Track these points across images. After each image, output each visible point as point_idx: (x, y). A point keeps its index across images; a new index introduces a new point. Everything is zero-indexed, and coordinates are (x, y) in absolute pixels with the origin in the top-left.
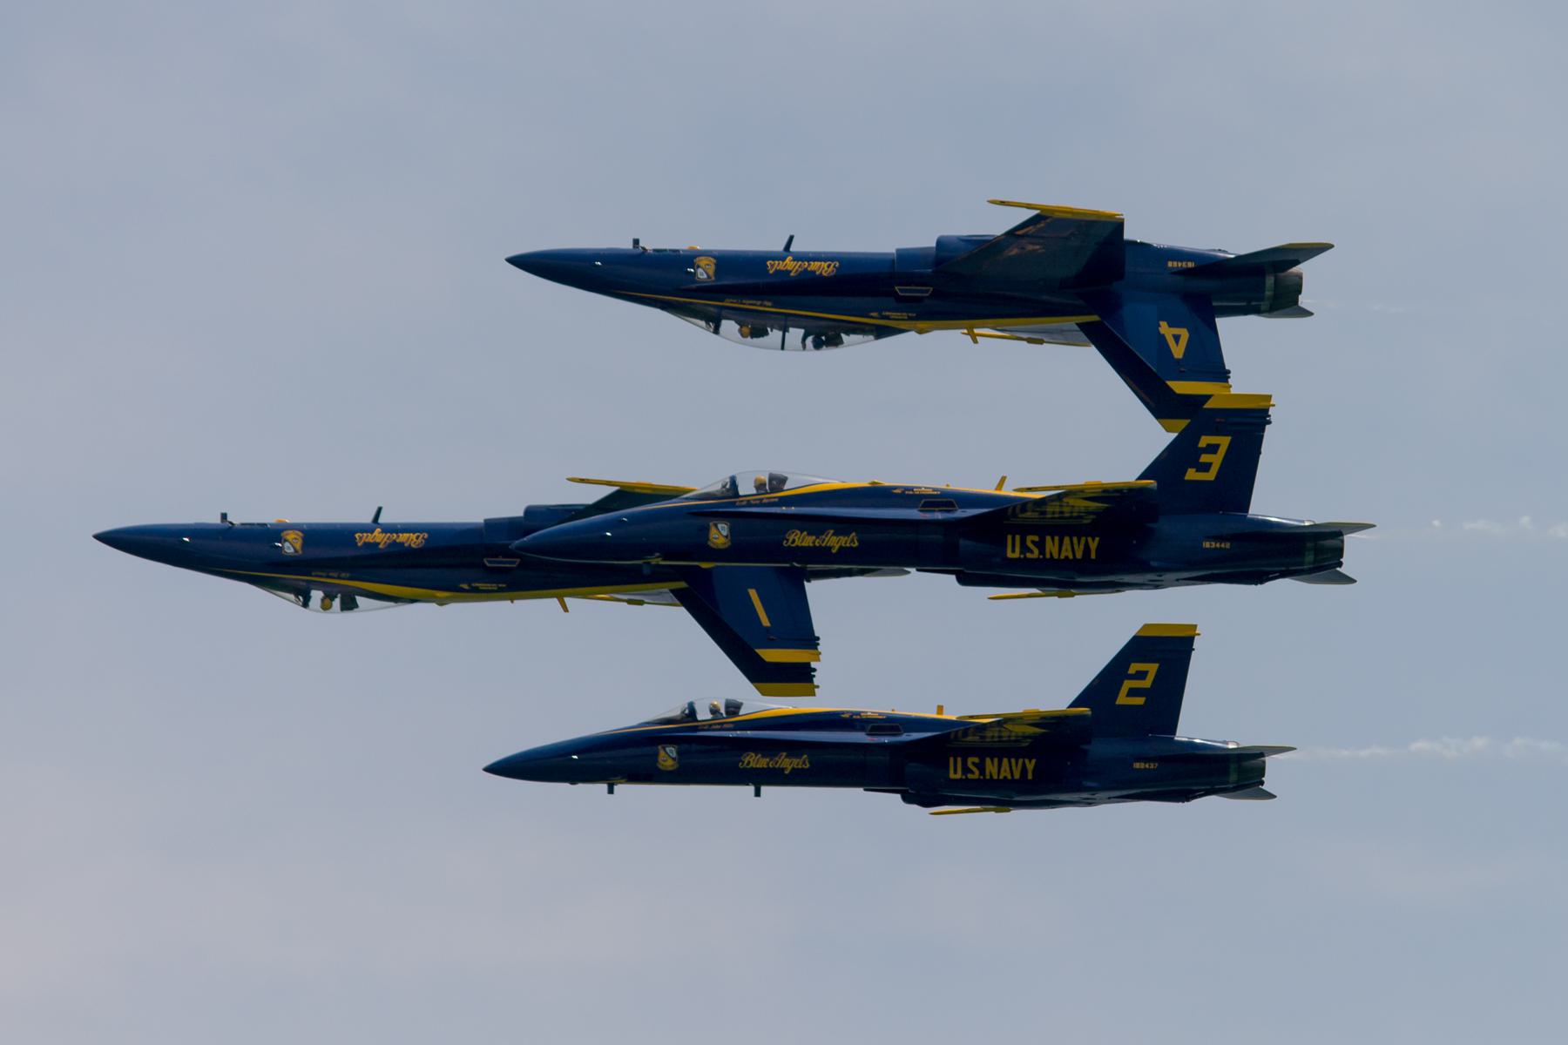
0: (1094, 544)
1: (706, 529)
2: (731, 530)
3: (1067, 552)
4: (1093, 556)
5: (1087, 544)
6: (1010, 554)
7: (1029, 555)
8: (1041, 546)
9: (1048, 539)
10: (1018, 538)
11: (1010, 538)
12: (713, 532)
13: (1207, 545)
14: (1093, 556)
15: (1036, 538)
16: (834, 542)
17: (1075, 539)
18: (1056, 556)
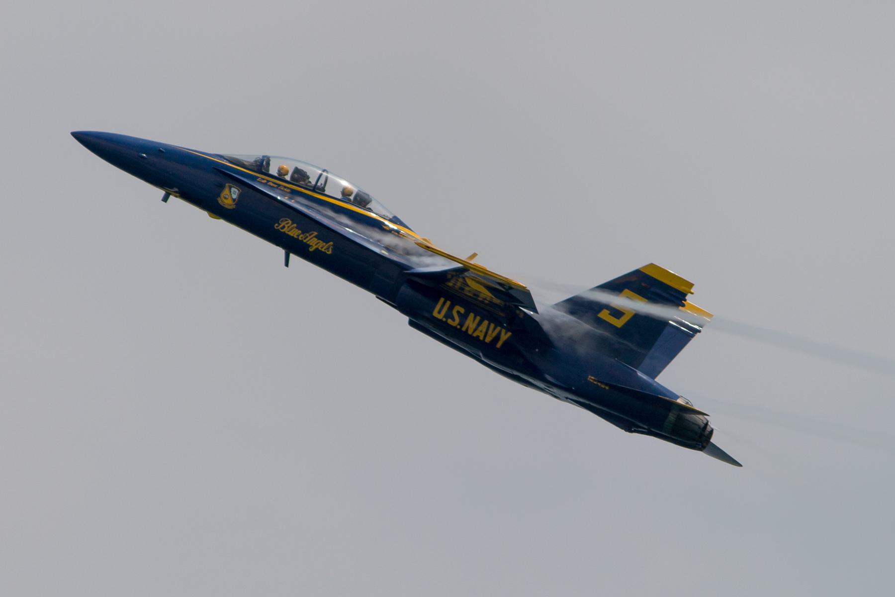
0: (505, 336)
1: (221, 187)
2: (240, 196)
3: (480, 334)
4: (499, 345)
5: (500, 333)
6: (435, 314)
7: (450, 321)
8: (463, 317)
9: (472, 315)
10: (448, 303)
11: (442, 300)
12: (226, 192)
13: (591, 378)
14: (499, 345)
15: (462, 310)
16: (314, 243)
17: (492, 325)
18: (470, 332)
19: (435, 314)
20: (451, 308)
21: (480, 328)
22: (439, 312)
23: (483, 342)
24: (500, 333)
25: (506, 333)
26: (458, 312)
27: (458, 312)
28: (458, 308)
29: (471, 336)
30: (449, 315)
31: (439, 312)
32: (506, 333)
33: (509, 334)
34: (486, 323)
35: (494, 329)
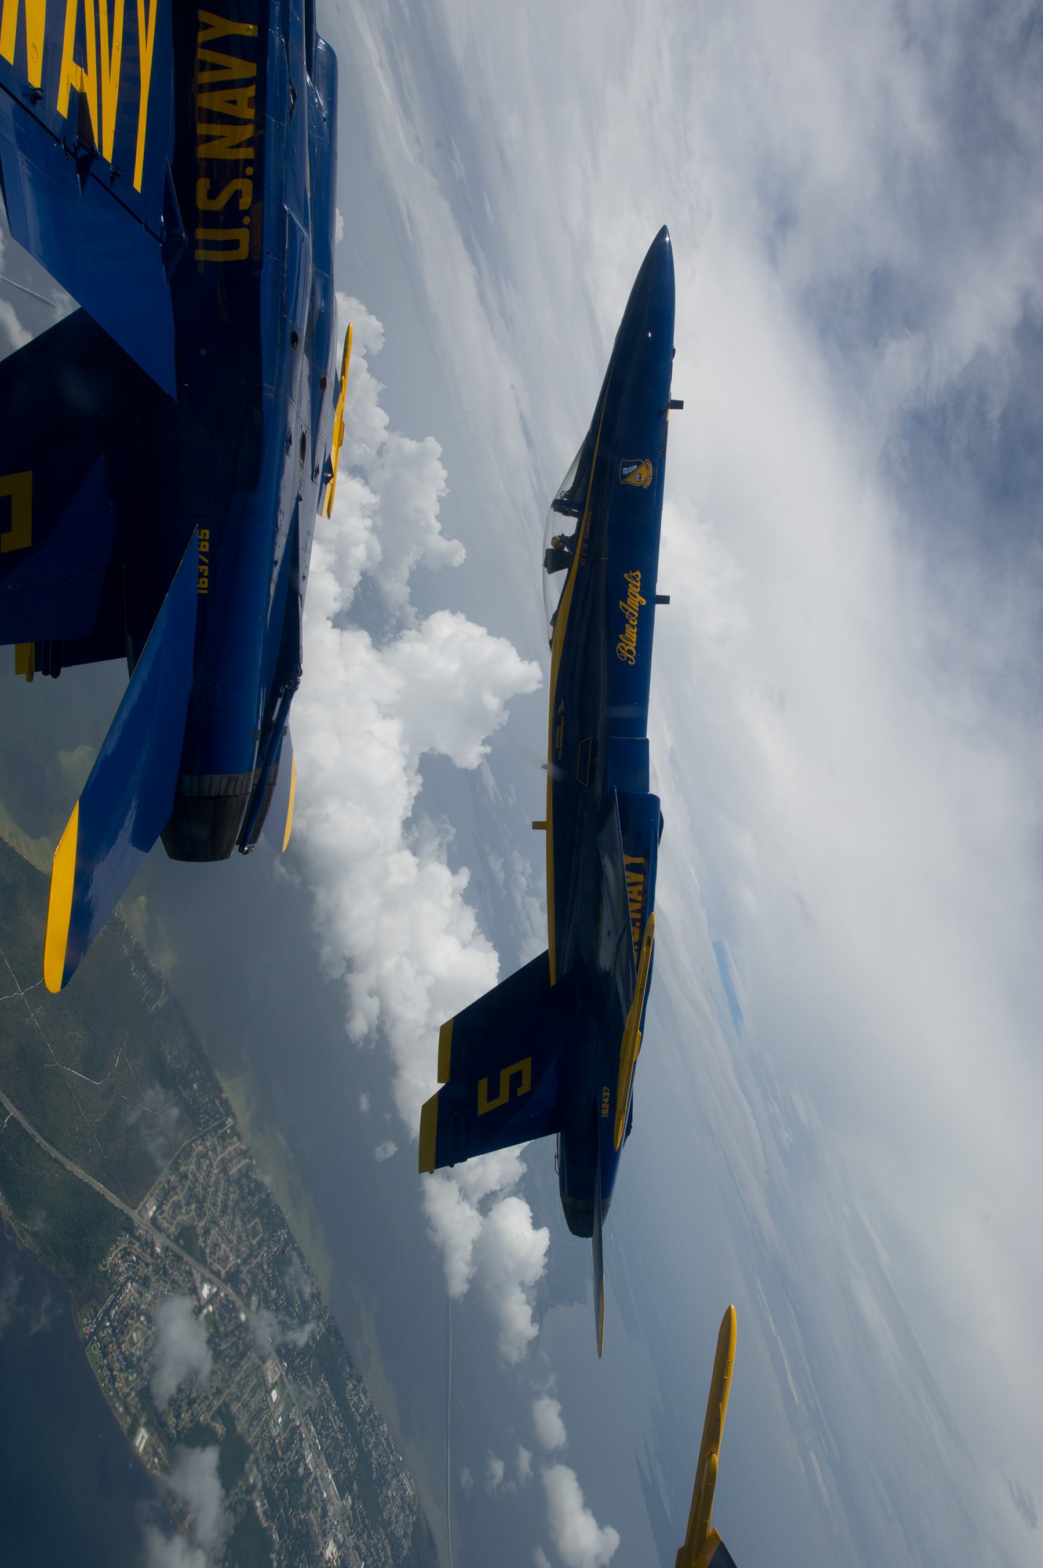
5: (209, 45)
9: (203, 151)
11: (202, 255)
15: (203, 185)
19: (242, 253)
20: (212, 220)
21: (229, 110)
22: (234, 245)
23: (260, 81)
24: (209, 45)
25: (207, 26)
26: (213, 194)
27: (213, 194)
28: (202, 202)
29: (260, 123)
30: (232, 216)
31: (234, 245)
32: (207, 26)
33: (204, 16)
34: (205, 100)
35: (203, 66)
